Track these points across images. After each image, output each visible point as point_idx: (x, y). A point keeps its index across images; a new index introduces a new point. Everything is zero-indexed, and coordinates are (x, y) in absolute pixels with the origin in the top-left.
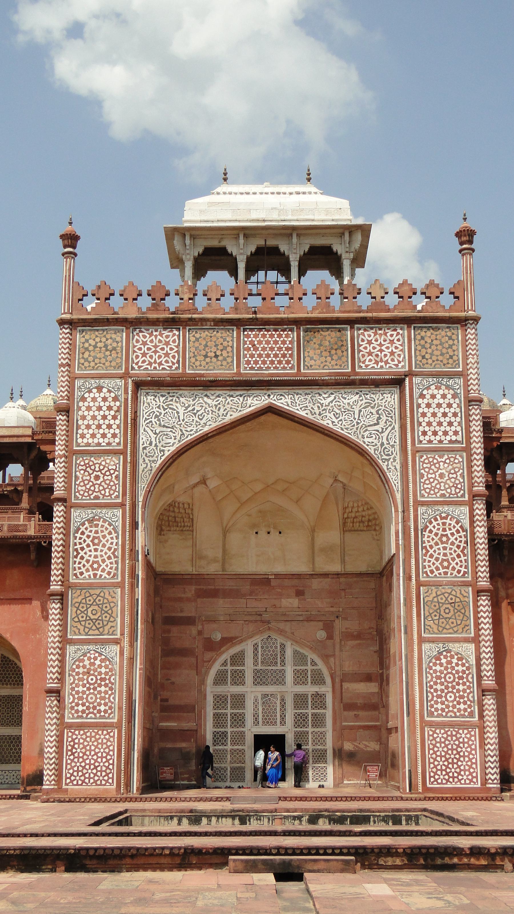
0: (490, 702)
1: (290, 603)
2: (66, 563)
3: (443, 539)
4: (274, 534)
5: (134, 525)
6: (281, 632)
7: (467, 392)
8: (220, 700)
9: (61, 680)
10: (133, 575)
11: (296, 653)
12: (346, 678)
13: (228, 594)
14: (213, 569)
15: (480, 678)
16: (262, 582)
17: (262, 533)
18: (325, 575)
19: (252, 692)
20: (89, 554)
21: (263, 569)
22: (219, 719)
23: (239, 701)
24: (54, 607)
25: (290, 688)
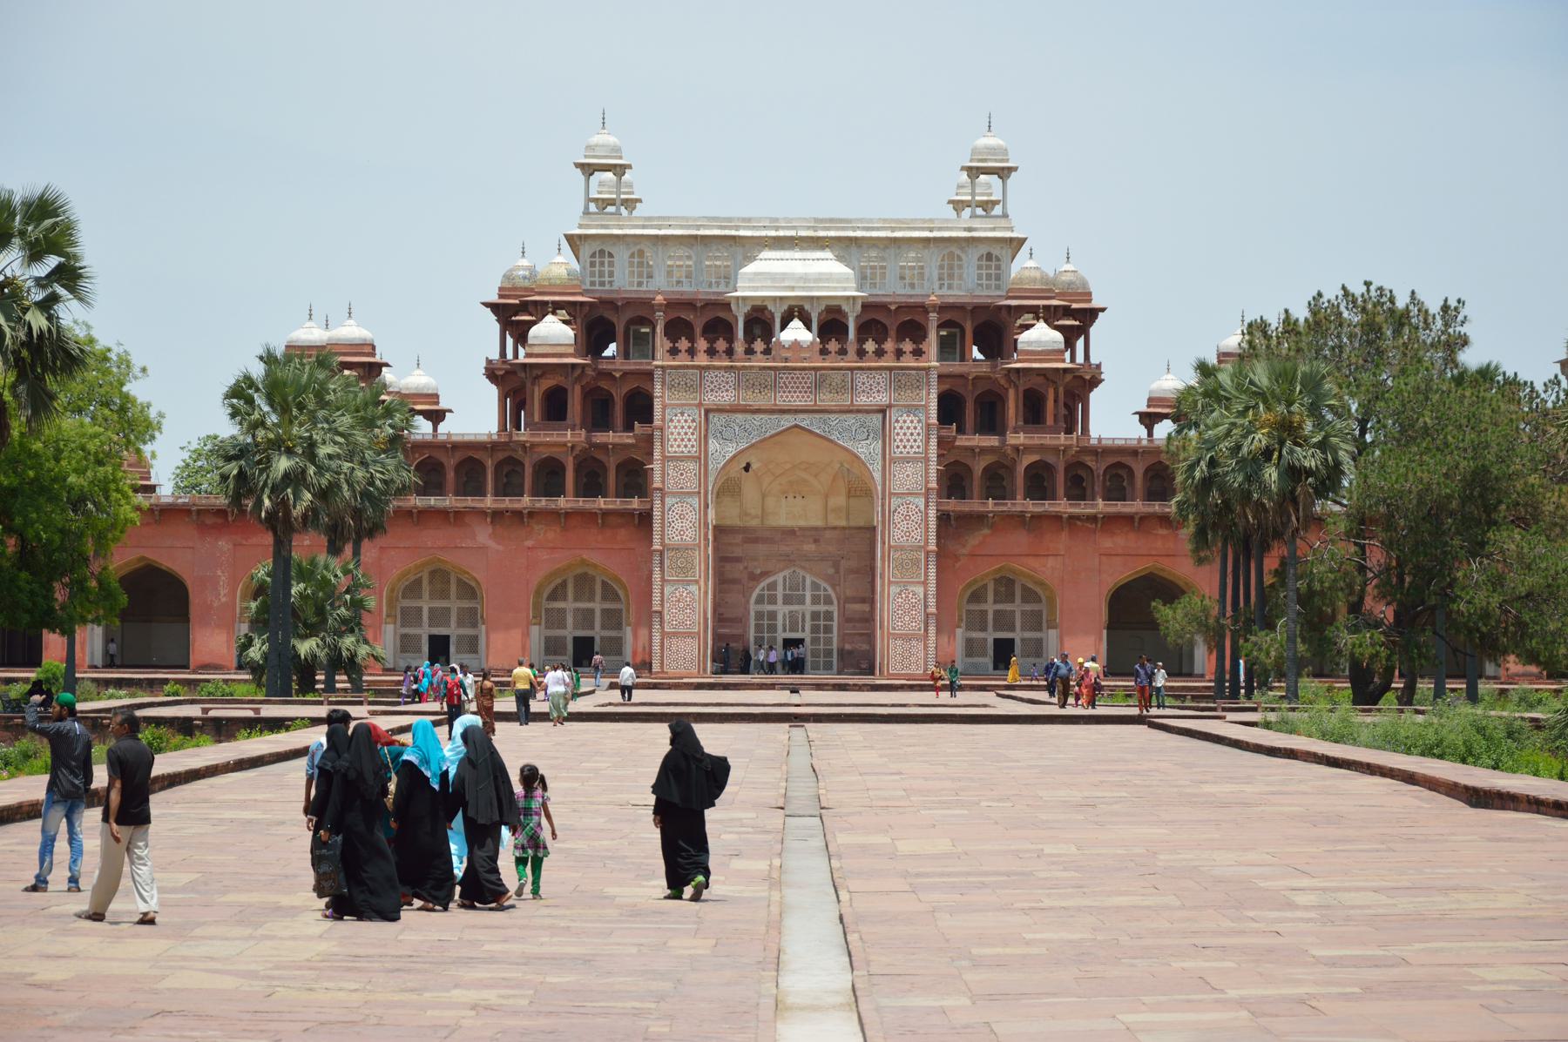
0: (932, 621)
1: (810, 547)
2: (663, 531)
3: (906, 517)
4: (799, 498)
5: (707, 506)
6: (803, 568)
7: (928, 418)
8: (759, 616)
9: (662, 605)
10: (706, 539)
11: (813, 583)
12: (849, 600)
13: (765, 540)
14: (755, 523)
15: (926, 607)
16: (791, 532)
17: (790, 498)
18: (835, 528)
19: (782, 610)
20: (678, 525)
21: (790, 523)
22: (759, 628)
23: (773, 616)
24: (657, 559)
25: (808, 607)
